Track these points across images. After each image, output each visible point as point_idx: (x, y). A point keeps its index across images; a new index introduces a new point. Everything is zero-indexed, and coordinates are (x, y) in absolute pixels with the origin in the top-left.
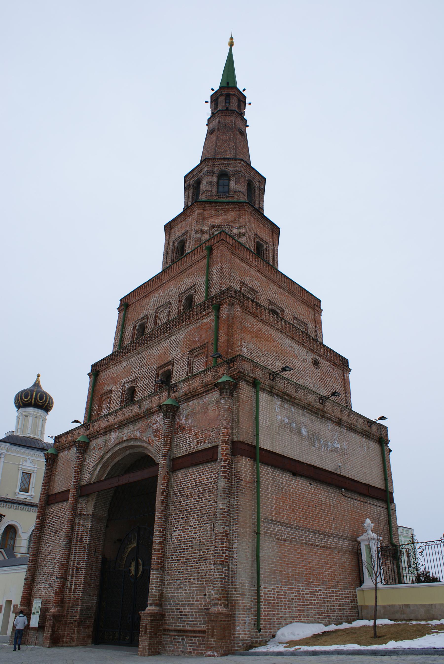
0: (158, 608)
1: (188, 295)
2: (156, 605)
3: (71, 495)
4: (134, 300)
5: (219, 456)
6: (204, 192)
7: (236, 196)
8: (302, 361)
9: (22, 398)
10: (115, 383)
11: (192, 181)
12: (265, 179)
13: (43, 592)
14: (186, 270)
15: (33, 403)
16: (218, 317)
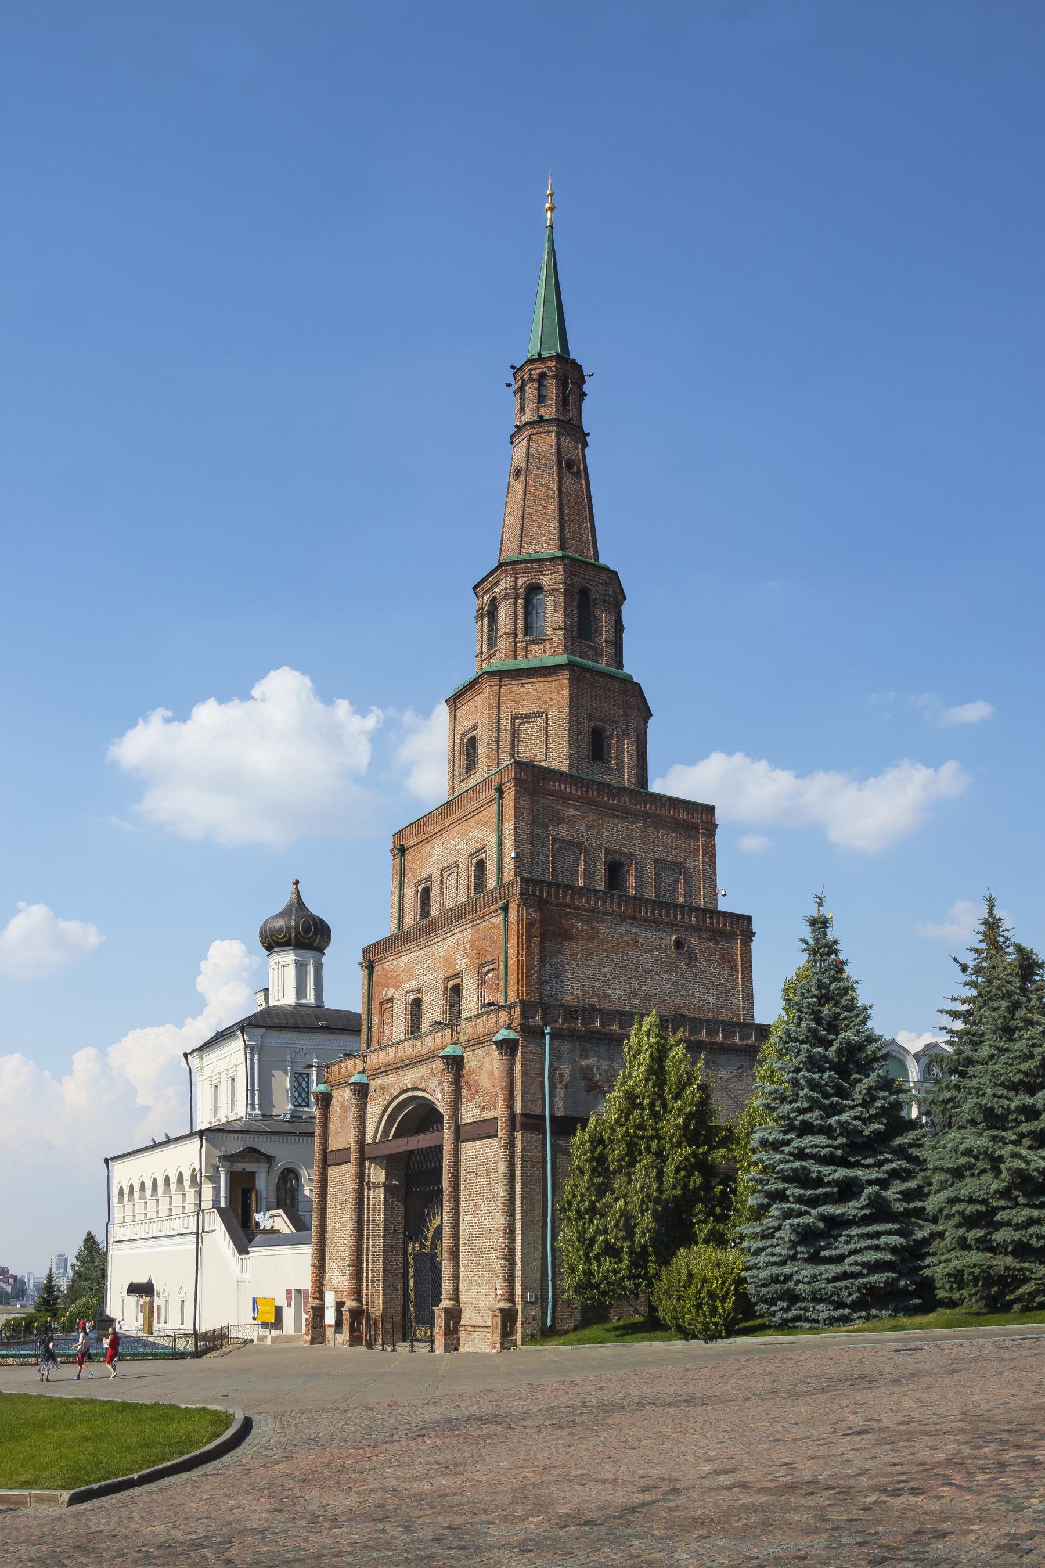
0: (453, 1303)
1: (479, 858)
2: (451, 1299)
3: (353, 1158)
4: (411, 843)
5: (499, 1134)
6: (501, 636)
7: (555, 638)
8: (651, 951)
9: (272, 935)
10: (397, 988)
11: (486, 598)
12: (616, 573)
13: (335, 1282)
14: (473, 813)
15: (293, 939)
16: (506, 921)
